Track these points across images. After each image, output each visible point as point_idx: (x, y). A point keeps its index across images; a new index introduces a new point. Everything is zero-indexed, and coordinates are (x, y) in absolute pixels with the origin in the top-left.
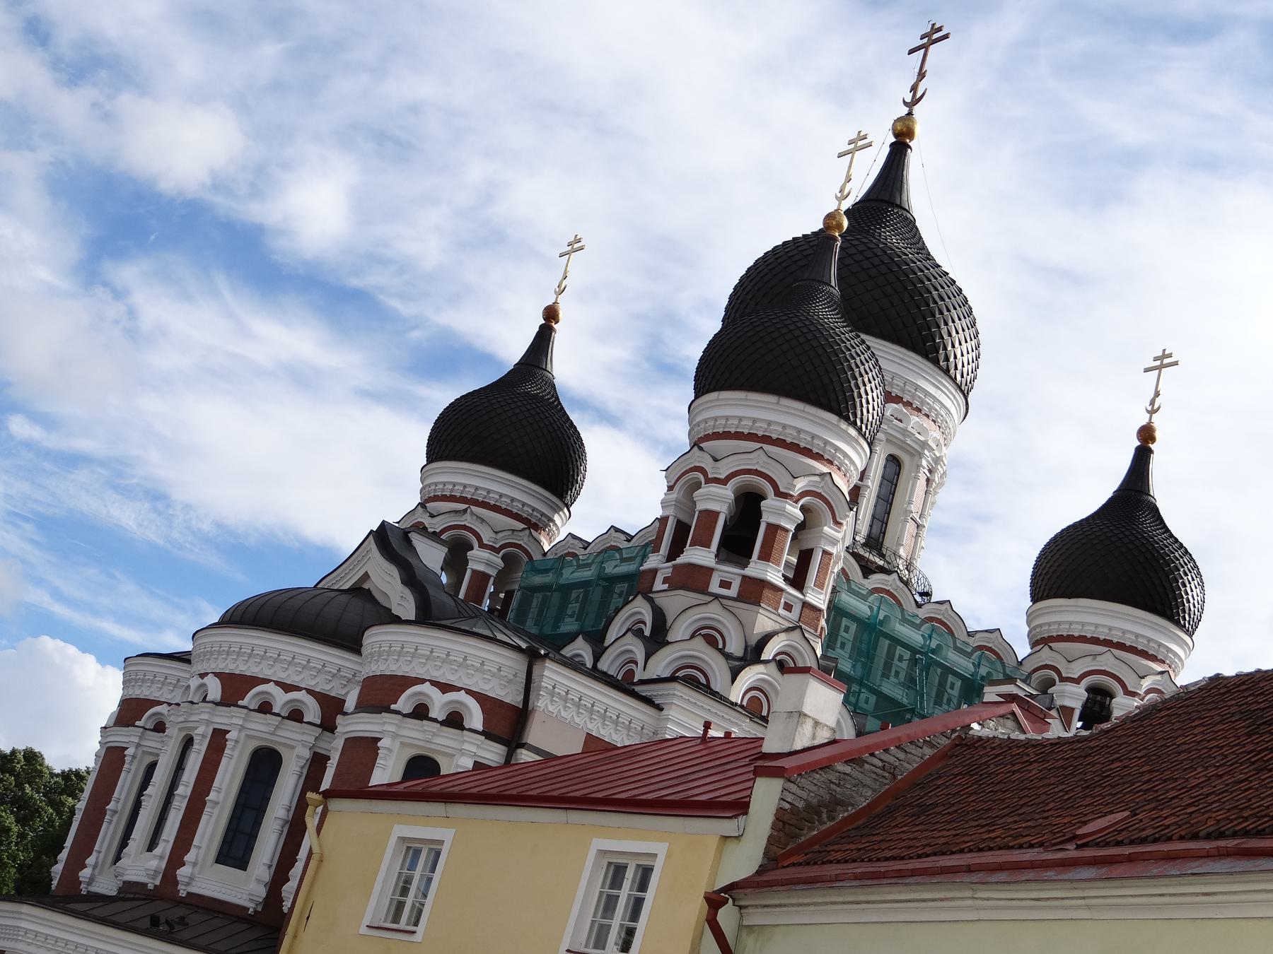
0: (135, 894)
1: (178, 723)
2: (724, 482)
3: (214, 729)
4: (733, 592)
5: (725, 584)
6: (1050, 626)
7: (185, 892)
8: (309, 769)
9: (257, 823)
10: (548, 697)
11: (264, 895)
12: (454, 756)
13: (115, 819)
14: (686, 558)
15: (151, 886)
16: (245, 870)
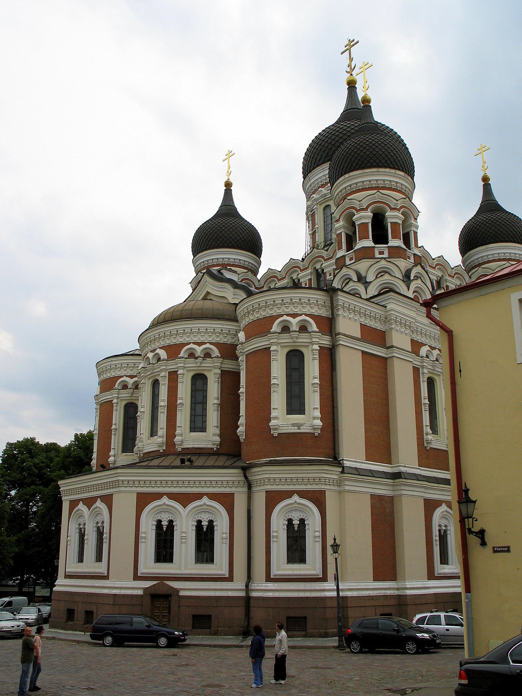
0: (153, 457)
1: (147, 376)
2: (366, 209)
3: (169, 372)
4: (386, 255)
5: (381, 253)
6: (478, 259)
7: (181, 449)
8: (221, 379)
9: (205, 409)
10: (342, 309)
11: (220, 440)
12: (309, 346)
13: (117, 433)
14: (358, 246)
15: (161, 451)
16: (519, 299)
